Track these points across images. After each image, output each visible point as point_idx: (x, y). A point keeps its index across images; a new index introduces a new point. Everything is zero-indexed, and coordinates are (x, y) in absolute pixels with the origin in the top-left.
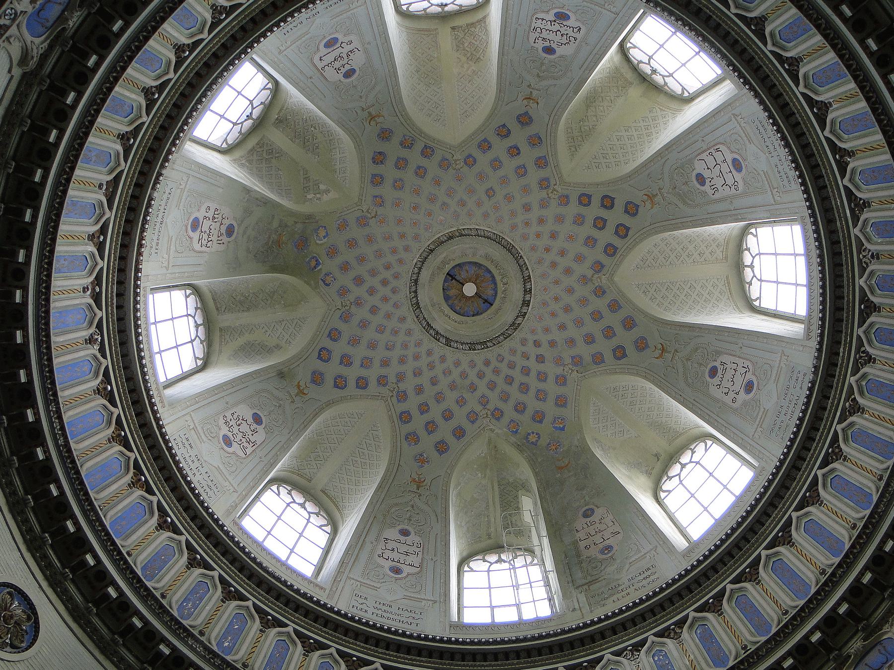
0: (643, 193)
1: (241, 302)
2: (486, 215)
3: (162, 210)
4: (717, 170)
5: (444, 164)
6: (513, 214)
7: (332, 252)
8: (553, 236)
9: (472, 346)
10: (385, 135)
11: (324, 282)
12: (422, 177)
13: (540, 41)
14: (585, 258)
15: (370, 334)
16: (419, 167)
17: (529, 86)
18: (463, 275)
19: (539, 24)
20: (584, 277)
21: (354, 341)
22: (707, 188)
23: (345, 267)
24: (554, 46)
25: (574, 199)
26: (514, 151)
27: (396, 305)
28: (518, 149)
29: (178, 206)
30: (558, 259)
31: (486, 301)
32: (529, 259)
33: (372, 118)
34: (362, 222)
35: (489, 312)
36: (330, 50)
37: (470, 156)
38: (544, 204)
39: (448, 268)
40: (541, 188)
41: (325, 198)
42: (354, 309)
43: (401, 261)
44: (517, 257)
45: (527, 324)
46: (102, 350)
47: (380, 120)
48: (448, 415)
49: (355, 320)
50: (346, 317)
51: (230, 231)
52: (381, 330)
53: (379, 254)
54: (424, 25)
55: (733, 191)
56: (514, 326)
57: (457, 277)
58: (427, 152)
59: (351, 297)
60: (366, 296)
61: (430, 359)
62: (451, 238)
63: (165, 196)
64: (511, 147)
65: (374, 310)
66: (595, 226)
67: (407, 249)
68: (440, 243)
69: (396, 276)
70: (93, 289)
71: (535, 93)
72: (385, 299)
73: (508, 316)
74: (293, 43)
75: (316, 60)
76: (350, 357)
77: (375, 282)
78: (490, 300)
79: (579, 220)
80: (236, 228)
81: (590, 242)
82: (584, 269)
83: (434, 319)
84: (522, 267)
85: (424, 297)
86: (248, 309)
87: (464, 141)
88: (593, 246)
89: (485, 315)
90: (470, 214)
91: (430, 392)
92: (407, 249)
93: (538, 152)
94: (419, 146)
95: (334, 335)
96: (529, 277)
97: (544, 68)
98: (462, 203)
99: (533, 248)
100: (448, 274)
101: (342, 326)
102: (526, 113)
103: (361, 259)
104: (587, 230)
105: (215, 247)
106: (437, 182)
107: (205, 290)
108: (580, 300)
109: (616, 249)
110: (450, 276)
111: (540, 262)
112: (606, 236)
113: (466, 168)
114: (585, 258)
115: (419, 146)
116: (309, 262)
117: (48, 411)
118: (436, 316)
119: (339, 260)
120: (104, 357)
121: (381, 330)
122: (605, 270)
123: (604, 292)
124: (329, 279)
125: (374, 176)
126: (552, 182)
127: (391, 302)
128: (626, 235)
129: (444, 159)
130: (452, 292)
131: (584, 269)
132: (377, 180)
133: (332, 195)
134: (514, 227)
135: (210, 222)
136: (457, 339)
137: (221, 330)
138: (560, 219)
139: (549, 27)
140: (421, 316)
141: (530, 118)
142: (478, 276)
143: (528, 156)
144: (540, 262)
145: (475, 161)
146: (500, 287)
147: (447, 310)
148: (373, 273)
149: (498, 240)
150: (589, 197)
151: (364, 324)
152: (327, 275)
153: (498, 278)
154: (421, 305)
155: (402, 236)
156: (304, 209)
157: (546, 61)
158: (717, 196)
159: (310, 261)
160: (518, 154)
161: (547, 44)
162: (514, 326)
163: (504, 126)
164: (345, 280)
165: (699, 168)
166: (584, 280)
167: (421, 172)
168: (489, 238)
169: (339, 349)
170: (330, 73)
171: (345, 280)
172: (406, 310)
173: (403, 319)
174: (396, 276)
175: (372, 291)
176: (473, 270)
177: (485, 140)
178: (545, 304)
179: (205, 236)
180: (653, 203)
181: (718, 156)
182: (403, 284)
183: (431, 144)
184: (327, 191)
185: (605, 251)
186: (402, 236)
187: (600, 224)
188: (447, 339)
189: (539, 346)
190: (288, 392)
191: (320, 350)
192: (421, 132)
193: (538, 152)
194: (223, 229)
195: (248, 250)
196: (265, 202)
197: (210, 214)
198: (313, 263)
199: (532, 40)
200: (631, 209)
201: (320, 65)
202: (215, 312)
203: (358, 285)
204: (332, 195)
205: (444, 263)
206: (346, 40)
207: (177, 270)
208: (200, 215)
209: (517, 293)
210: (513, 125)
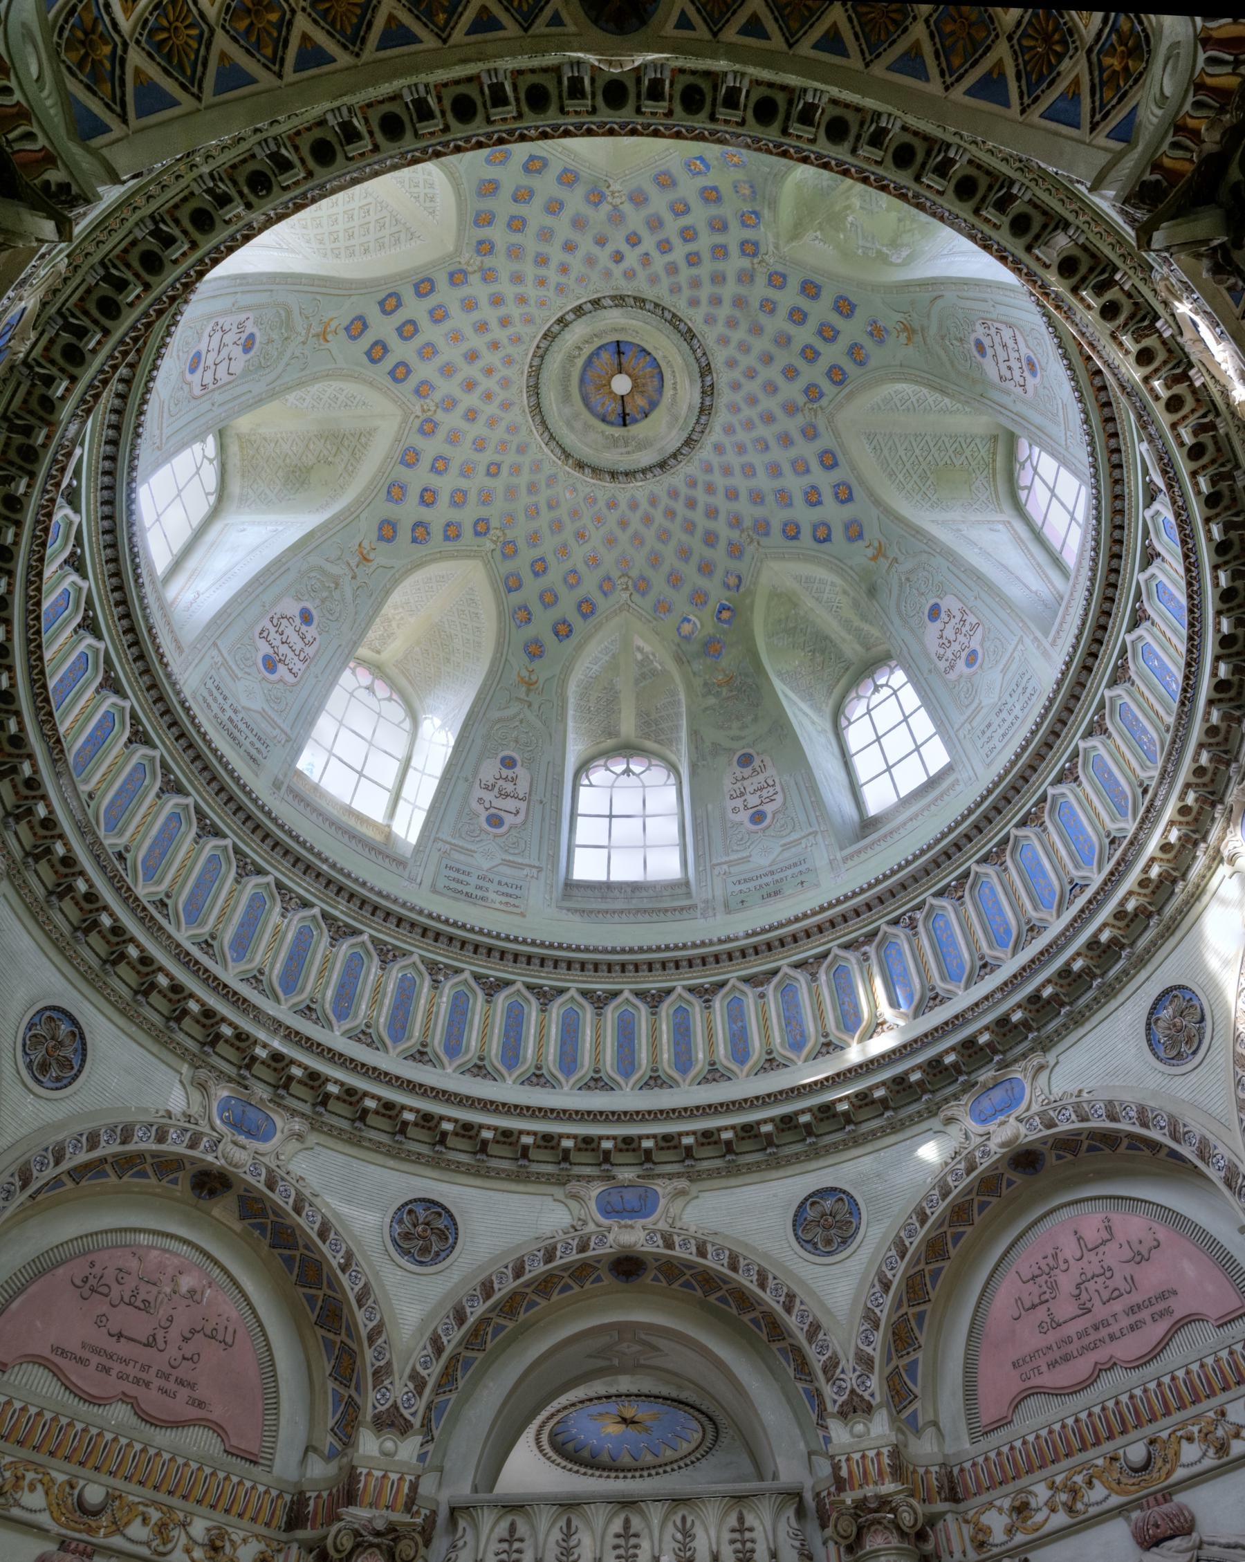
0: (327, 345)
1: (823, 651)
2: (522, 449)
3: (757, 883)
4: (224, 353)
5: (509, 550)
6: (492, 422)
7: (698, 598)
8: (472, 356)
9: (689, 336)
10: (534, 650)
11: (738, 587)
12: (542, 559)
13: (309, 638)
14: (462, 301)
15: (763, 481)
16: (536, 574)
17: (354, 577)
18: (613, 408)
19: (298, 666)
20: (484, 280)
21: (784, 498)
22: (250, 328)
23: (706, 569)
24: (298, 621)
25: (413, 382)
26: (428, 497)
27: (708, 469)
28: (422, 497)
29: (746, 860)
30: (494, 324)
31: (619, 353)
32: (524, 355)
33: (530, 685)
34: (642, 586)
35: (629, 339)
36: (502, 814)
37: (477, 534)
38: (449, 404)
39: (618, 432)
40: (436, 425)
41: (647, 648)
42: (748, 523)
43: (653, 501)
44: (536, 373)
45: (605, 290)
46: (919, 907)
47: (524, 673)
48: (798, 317)
49: (759, 512)
50: (763, 528)
51: (746, 760)
52: (749, 470)
53: (664, 536)
54: (403, 682)
55: (221, 322)
56: (619, 300)
57: (620, 410)
58: (512, 584)
59: (735, 535)
60: (722, 517)
61: (743, 380)
62: (581, 465)
63: (744, 887)
64: (428, 505)
65: (732, 495)
66: (416, 330)
67: (634, 506)
68: (596, 471)
69: (673, 494)
70: (864, 944)
71: (353, 563)
72: (710, 489)
73: (613, 317)
74: (521, 866)
75: (521, 817)
76: (806, 493)
77: (698, 516)
78: (613, 348)
79: (428, 351)
80: (739, 754)
81: (439, 315)
82: (477, 289)
83: (690, 407)
84: (541, 355)
85: (673, 441)
86: (826, 638)
87: (468, 557)
88: (440, 306)
89: (636, 341)
90: (537, 467)
91: (784, 358)
92: (634, 506)
93: (404, 474)
94: (516, 598)
95: (792, 532)
96: (545, 336)
97: (325, 594)
98: (532, 488)
99: (509, 361)
100: (625, 425)
101: (776, 527)
102: (381, 538)
103: (685, 554)
104: (430, 332)
105: (771, 772)
106: (534, 539)
107: (831, 703)
108: (517, 257)
109: (417, 286)
110: (624, 420)
111: (516, 340)
112: (415, 308)
113: (494, 523)
114: (462, 301)
115: (516, 598)
116: (728, 622)
117: (975, 1018)
118: (685, 407)
119: (702, 582)
120: (924, 902)
121: (749, 470)
122: (451, 269)
123: (480, 243)
124: (732, 581)
125: (585, 616)
126: (417, 423)
127: (708, 478)
128: (390, 295)
129: (505, 556)
130: (641, 401)
131: (477, 289)
132: (587, 608)
133: (639, 642)
134: (506, 406)
135: (748, 797)
136: (692, 360)
137: (868, 649)
138: (448, 370)
139: (290, 654)
140: (698, 429)
141: (380, 529)
142: (599, 388)
143: (418, 478)
144: (516, 340)
145: (476, 523)
146: (588, 350)
147: (668, 392)
148: (690, 527)
149: (537, 409)
150: (392, 373)
151: (757, 498)
152: (728, 587)
153: (580, 362)
154: (685, 435)
155: (623, 524)
156: (672, 667)
157: (317, 602)
158: (243, 317)
159: (725, 622)
160: (425, 490)
161: (304, 628)
162: (619, 300)
163: (414, 540)
164: (719, 555)
165: (240, 361)
166: (488, 276)
167: (539, 568)
168: (543, 422)
169: (804, 515)
170: (522, 788)
171: (719, 555)
172: (705, 452)
173: (719, 449)
174: (673, 494)
175: (712, 513)
176: (595, 399)
177: (447, 538)
178: (560, 289)
179: (765, 793)
180: (328, 324)
181: (208, 379)
182: (676, 478)
183: (502, 588)
184: (639, 649)
185: (432, 290)
186: (623, 524)
187: (408, 330)
188: (702, 376)
189: (618, 252)
190: (888, 572)
191: (819, 541)
192: (500, 614)
193: (404, 474)
194: (747, 771)
195: (755, 719)
196: (694, 734)
197: (739, 803)
198: (725, 615)
199: (316, 644)
200: (358, 326)
201: (523, 806)
202: (852, 668)
203: (717, 537)
204: (639, 642)
205: (615, 442)
206: (479, 808)
207: (813, 820)
208: (744, 816)
209: (578, 331)
210: (404, 534)
